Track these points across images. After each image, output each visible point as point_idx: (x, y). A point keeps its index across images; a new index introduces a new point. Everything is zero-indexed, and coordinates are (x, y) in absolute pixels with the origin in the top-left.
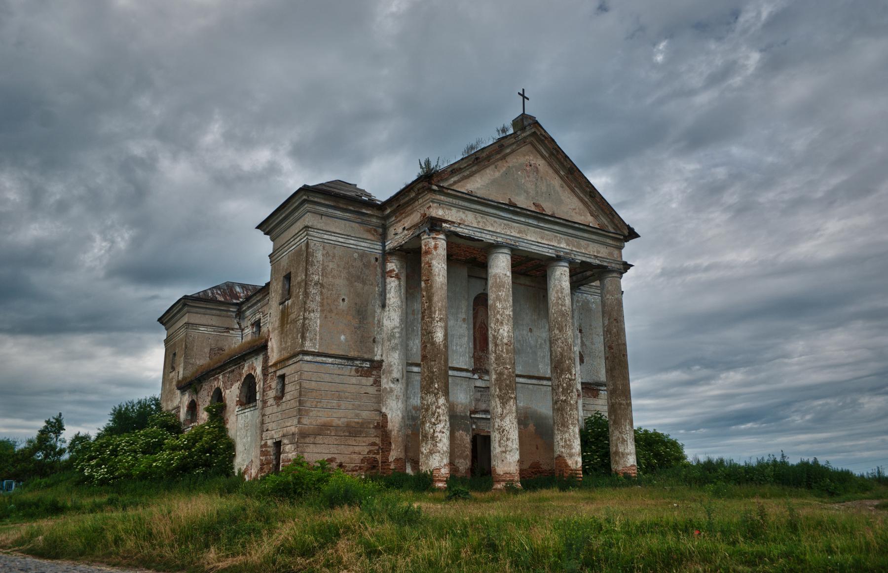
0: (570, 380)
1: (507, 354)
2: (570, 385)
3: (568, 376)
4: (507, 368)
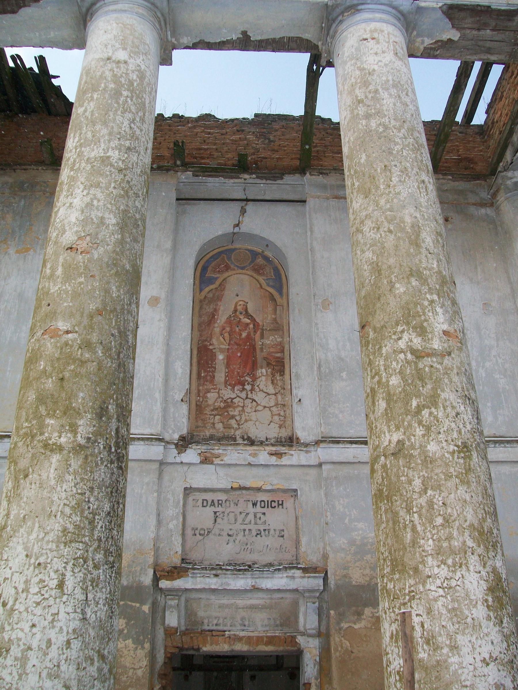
0: (418, 355)
1: (67, 278)
2: (420, 376)
3: (410, 339)
4: (55, 334)
